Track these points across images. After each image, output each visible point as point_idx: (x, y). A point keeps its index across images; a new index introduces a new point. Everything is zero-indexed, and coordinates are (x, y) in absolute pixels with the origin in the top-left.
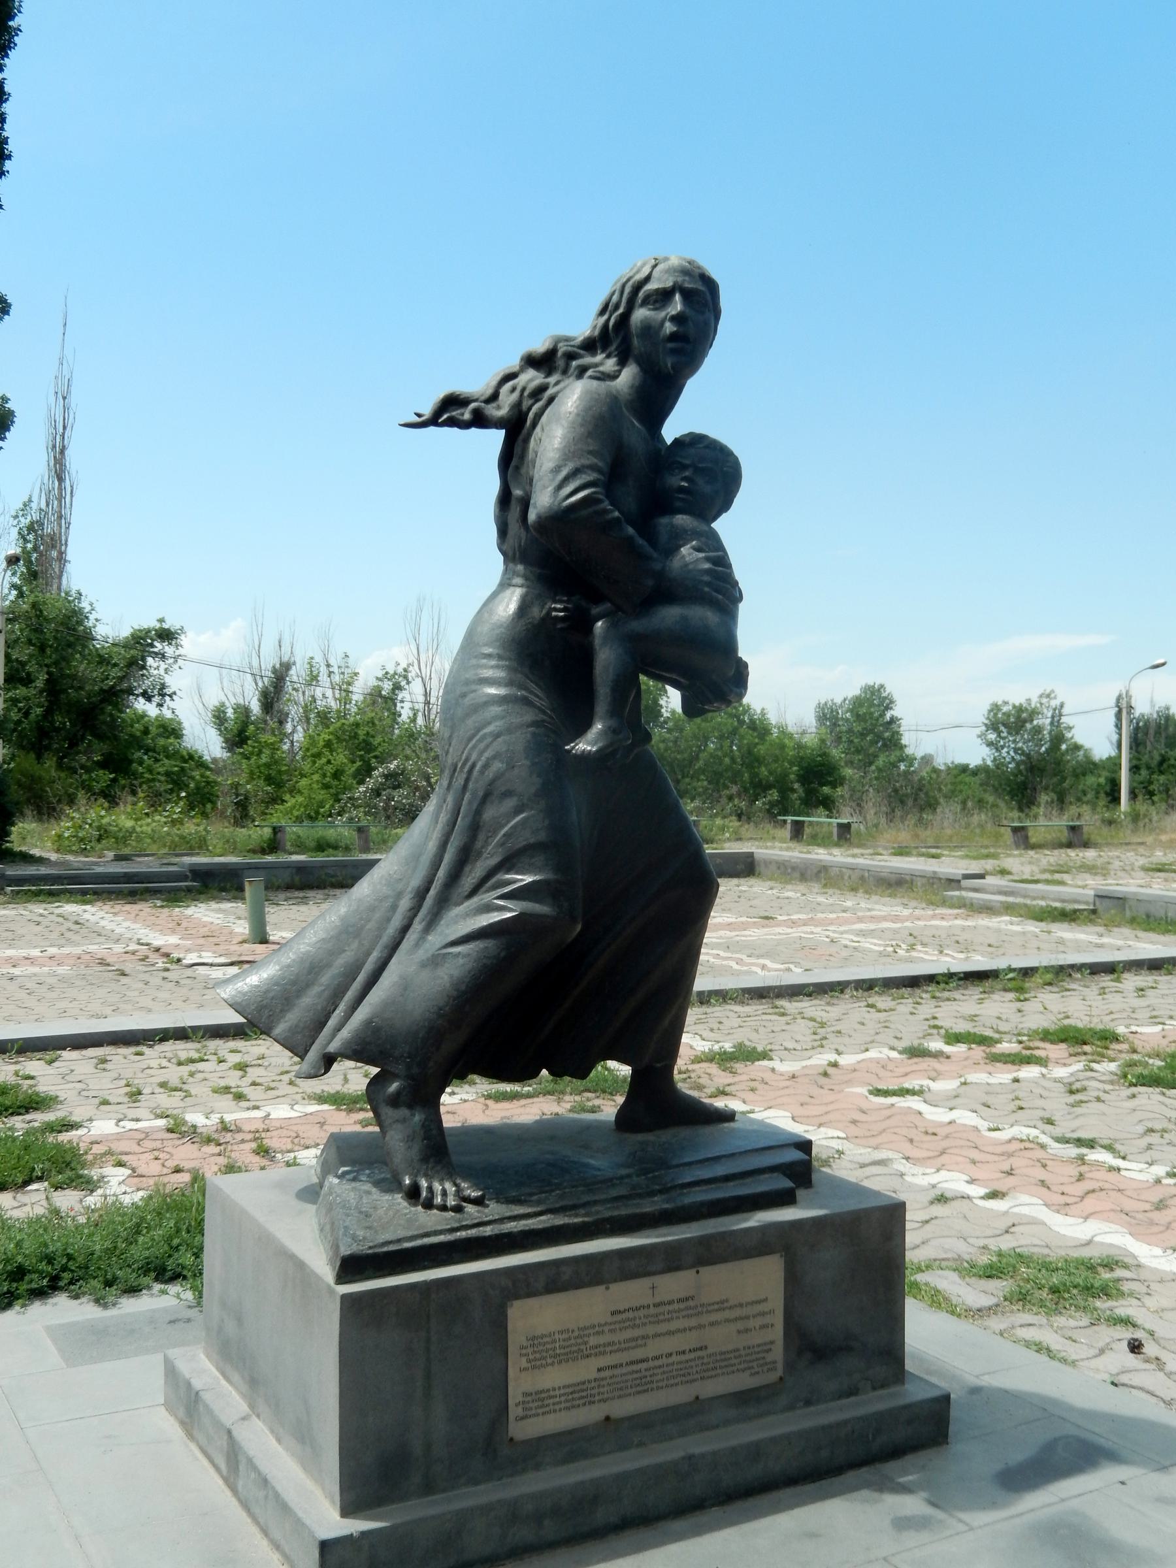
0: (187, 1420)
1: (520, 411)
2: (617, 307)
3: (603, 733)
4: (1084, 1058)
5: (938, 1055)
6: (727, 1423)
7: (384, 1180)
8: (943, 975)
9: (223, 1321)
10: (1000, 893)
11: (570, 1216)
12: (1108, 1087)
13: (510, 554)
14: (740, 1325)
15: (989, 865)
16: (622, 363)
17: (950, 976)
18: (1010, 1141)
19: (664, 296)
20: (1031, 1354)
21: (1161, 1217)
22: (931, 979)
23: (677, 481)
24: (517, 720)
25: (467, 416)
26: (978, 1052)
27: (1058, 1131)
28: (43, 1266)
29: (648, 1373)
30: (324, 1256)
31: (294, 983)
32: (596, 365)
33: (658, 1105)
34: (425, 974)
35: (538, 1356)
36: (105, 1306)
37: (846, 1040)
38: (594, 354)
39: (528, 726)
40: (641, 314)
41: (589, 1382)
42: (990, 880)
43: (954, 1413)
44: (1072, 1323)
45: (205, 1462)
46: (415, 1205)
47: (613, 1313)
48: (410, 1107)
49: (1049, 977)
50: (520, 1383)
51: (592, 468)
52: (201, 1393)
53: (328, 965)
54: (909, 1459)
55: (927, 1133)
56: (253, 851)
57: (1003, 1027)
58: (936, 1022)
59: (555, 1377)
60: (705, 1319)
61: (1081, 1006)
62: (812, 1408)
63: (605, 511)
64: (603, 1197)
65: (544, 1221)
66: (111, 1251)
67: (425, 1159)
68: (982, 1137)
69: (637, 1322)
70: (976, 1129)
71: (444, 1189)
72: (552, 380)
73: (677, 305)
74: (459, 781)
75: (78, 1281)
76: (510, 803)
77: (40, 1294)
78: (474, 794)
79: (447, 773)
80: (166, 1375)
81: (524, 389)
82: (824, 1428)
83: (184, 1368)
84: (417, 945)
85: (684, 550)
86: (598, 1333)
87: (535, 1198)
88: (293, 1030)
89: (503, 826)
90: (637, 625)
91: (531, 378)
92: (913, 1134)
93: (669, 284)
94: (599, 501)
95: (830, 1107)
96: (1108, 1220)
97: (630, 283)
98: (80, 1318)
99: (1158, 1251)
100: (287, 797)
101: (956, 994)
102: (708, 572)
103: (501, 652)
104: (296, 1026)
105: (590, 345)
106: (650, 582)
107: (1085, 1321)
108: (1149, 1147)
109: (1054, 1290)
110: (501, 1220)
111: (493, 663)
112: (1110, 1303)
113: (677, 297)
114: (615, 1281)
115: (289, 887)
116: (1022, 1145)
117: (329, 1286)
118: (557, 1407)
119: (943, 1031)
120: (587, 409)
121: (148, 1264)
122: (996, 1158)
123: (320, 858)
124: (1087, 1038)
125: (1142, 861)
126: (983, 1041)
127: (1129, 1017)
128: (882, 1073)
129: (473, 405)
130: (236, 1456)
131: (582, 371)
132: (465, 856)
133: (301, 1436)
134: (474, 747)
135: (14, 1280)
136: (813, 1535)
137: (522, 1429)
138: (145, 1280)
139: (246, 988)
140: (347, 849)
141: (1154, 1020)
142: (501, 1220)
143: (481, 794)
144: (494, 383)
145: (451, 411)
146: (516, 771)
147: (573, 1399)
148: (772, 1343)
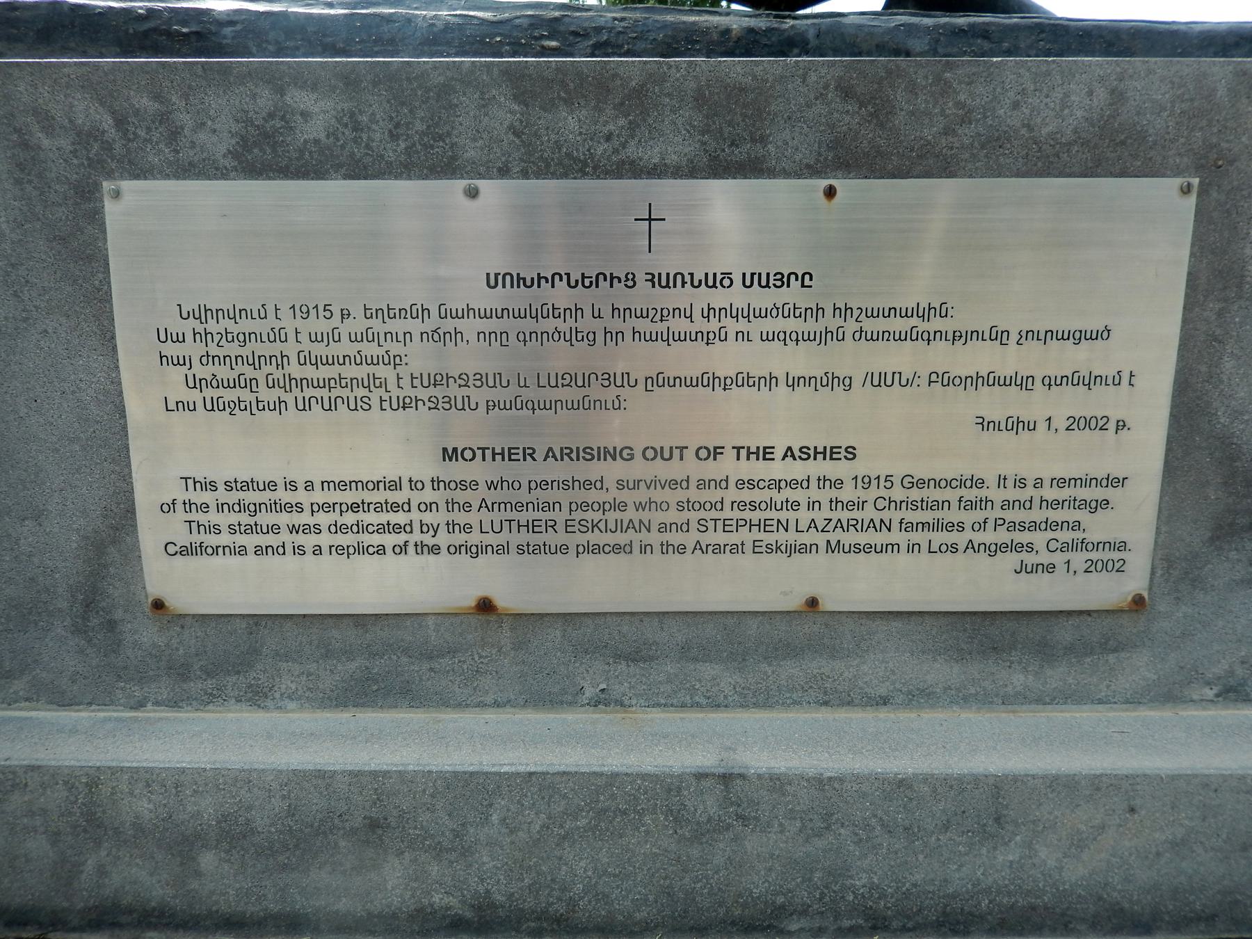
6: (920, 697)
14: (995, 404)
60: (851, 358)
69: (586, 323)
147: (361, 528)
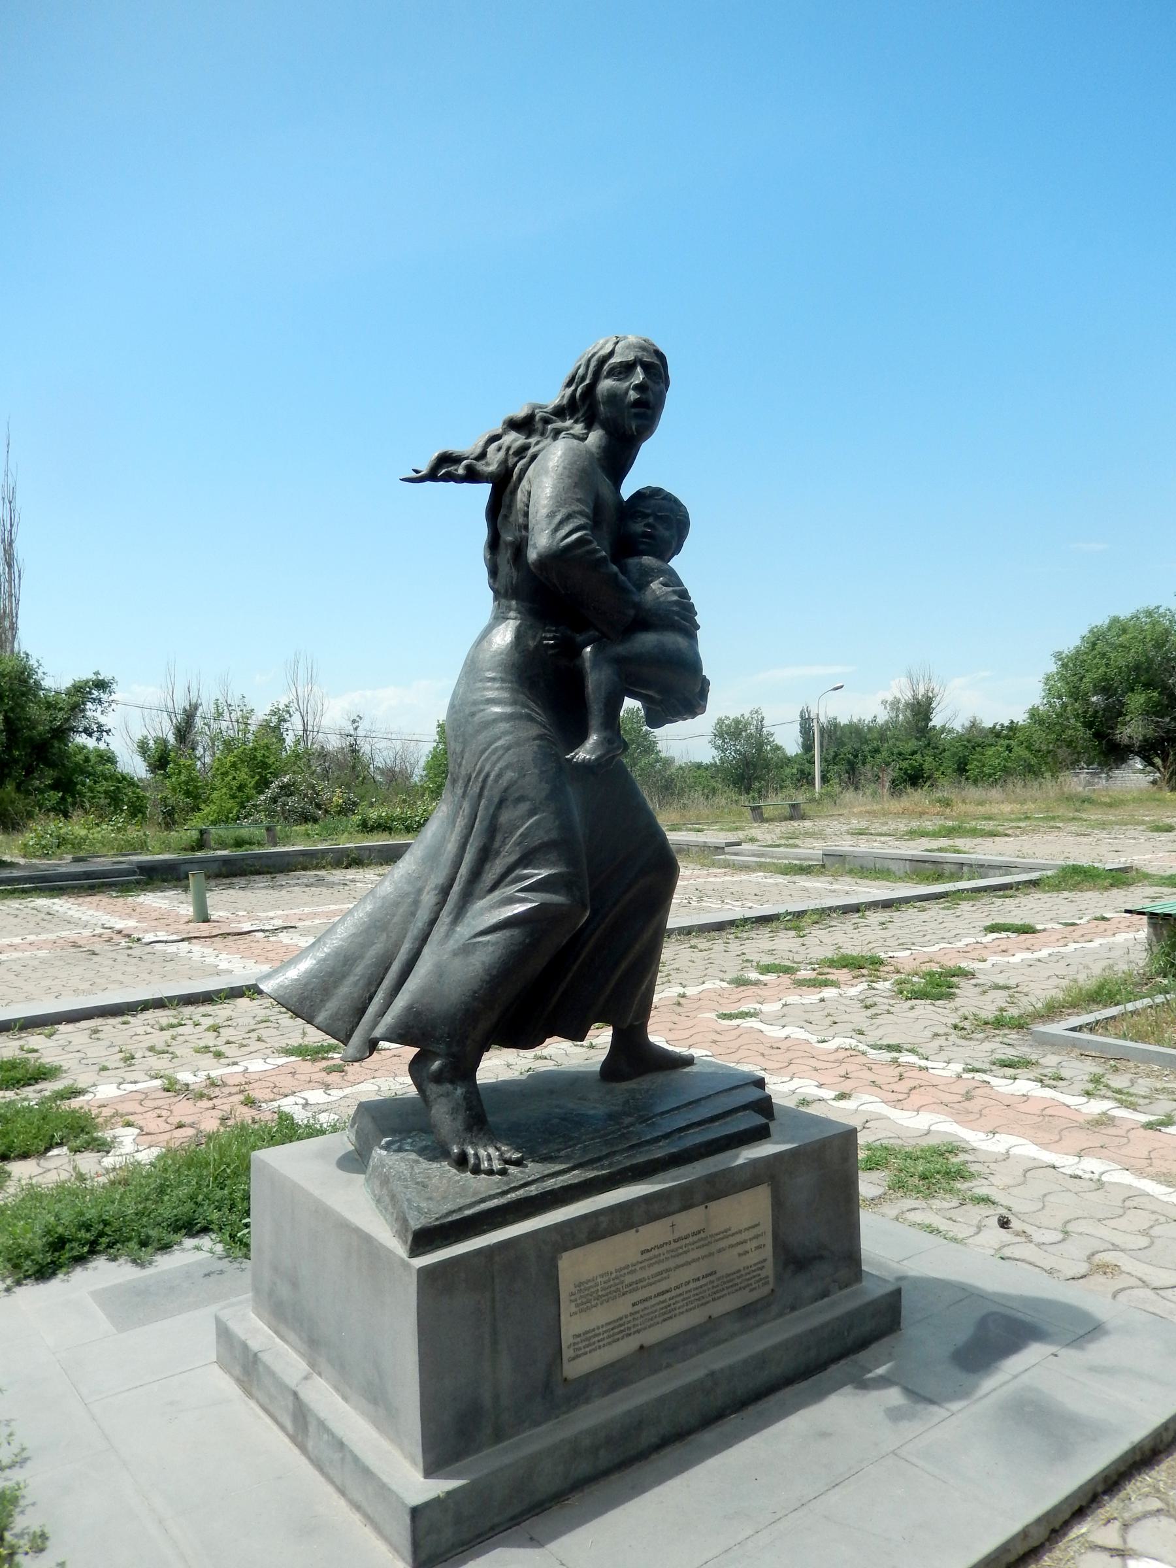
0: (245, 1379)
1: (507, 467)
2: (583, 378)
3: (596, 743)
4: (864, 979)
5: (757, 983)
6: (733, 1335)
7: (425, 1148)
8: (741, 920)
9: (275, 1284)
10: (754, 855)
11: (597, 1169)
12: (892, 1002)
13: (502, 591)
14: (740, 1249)
15: (741, 835)
16: (589, 427)
17: (745, 921)
18: (837, 1050)
19: (626, 369)
20: (925, 1235)
21: (972, 1105)
22: (732, 923)
23: (638, 527)
24: (524, 734)
25: (461, 471)
26: (786, 979)
27: (870, 1040)
28: (83, 1234)
29: (672, 1302)
30: (388, 1228)
31: (331, 974)
32: (567, 429)
33: (634, 1057)
34: (457, 962)
35: (584, 1300)
36: (142, 1266)
37: (685, 975)
38: (564, 420)
39: (534, 739)
40: (606, 384)
41: (626, 1316)
42: (745, 846)
43: (905, 1302)
44: (946, 1205)
45: (268, 1421)
46: (464, 1171)
47: (642, 1253)
48: (452, 1082)
49: (815, 917)
50: (572, 1325)
51: (581, 513)
52: (260, 1354)
53: (361, 957)
54: (875, 1348)
55: (772, 1047)
56: (185, 850)
57: (798, 958)
58: (746, 957)
59: (599, 1317)
60: (714, 1248)
61: (847, 938)
62: (797, 1313)
63: (595, 551)
64: (620, 1147)
65: (578, 1175)
66: (140, 1214)
67: (469, 1128)
68: (814, 1048)
69: (662, 1257)
70: (808, 1042)
71: (488, 1154)
72: (533, 440)
73: (639, 376)
74: (474, 789)
75: (114, 1244)
76: (524, 807)
77: (80, 1260)
78: (490, 800)
79: (460, 783)
80: (219, 1335)
81: (509, 448)
82: (812, 1331)
83: (238, 1329)
84: (448, 936)
85: (654, 585)
86: (630, 1273)
87: (563, 1153)
88: (334, 1017)
89: (518, 828)
90: (620, 649)
91: (513, 439)
92: (761, 1048)
93: (631, 358)
94: (590, 542)
95: (692, 1031)
96: (933, 1111)
97: (596, 357)
98: (120, 1280)
99: (982, 1136)
100: (203, 806)
101: (752, 934)
102: (676, 603)
103: (499, 675)
104: (337, 1013)
105: (560, 412)
106: (632, 612)
107: (955, 1203)
108: (941, 1049)
109: (924, 1177)
110: (542, 1179)
111: (497, 685)
112: (967, 1185)
113: (639, 369)
114: (643, 1224)
115: (218, 876)
116: (849, 1053)
117: (403, 1260)
118: (601, 1344)
119: (754, 964)
120: (572, 463)
121: (177, 1221)
122: (832, 1065)
123: (240, 852)
124: (862, 963)
125: (845, 828)
126: (787, 970)
127: (883, 946)
128: (721, 1001)
129: (465, 462)
130: (305, 1417)
131: (557, 433)
132: (485, 855)
133: (374, 1397)
134: (487, 759)
135: (55, 1250)
136: (824, 1435)
137: (574, 1369)
138: (176, 1237)
139: (287, 982)
140: (260, 844)
141: (902, 946)
142: (542, 1179)
143: (496, 800)
144: (482, 443)
145: (445, 468)
146: (527, 779)
147: (614, 1335)
148: (765, 1260)
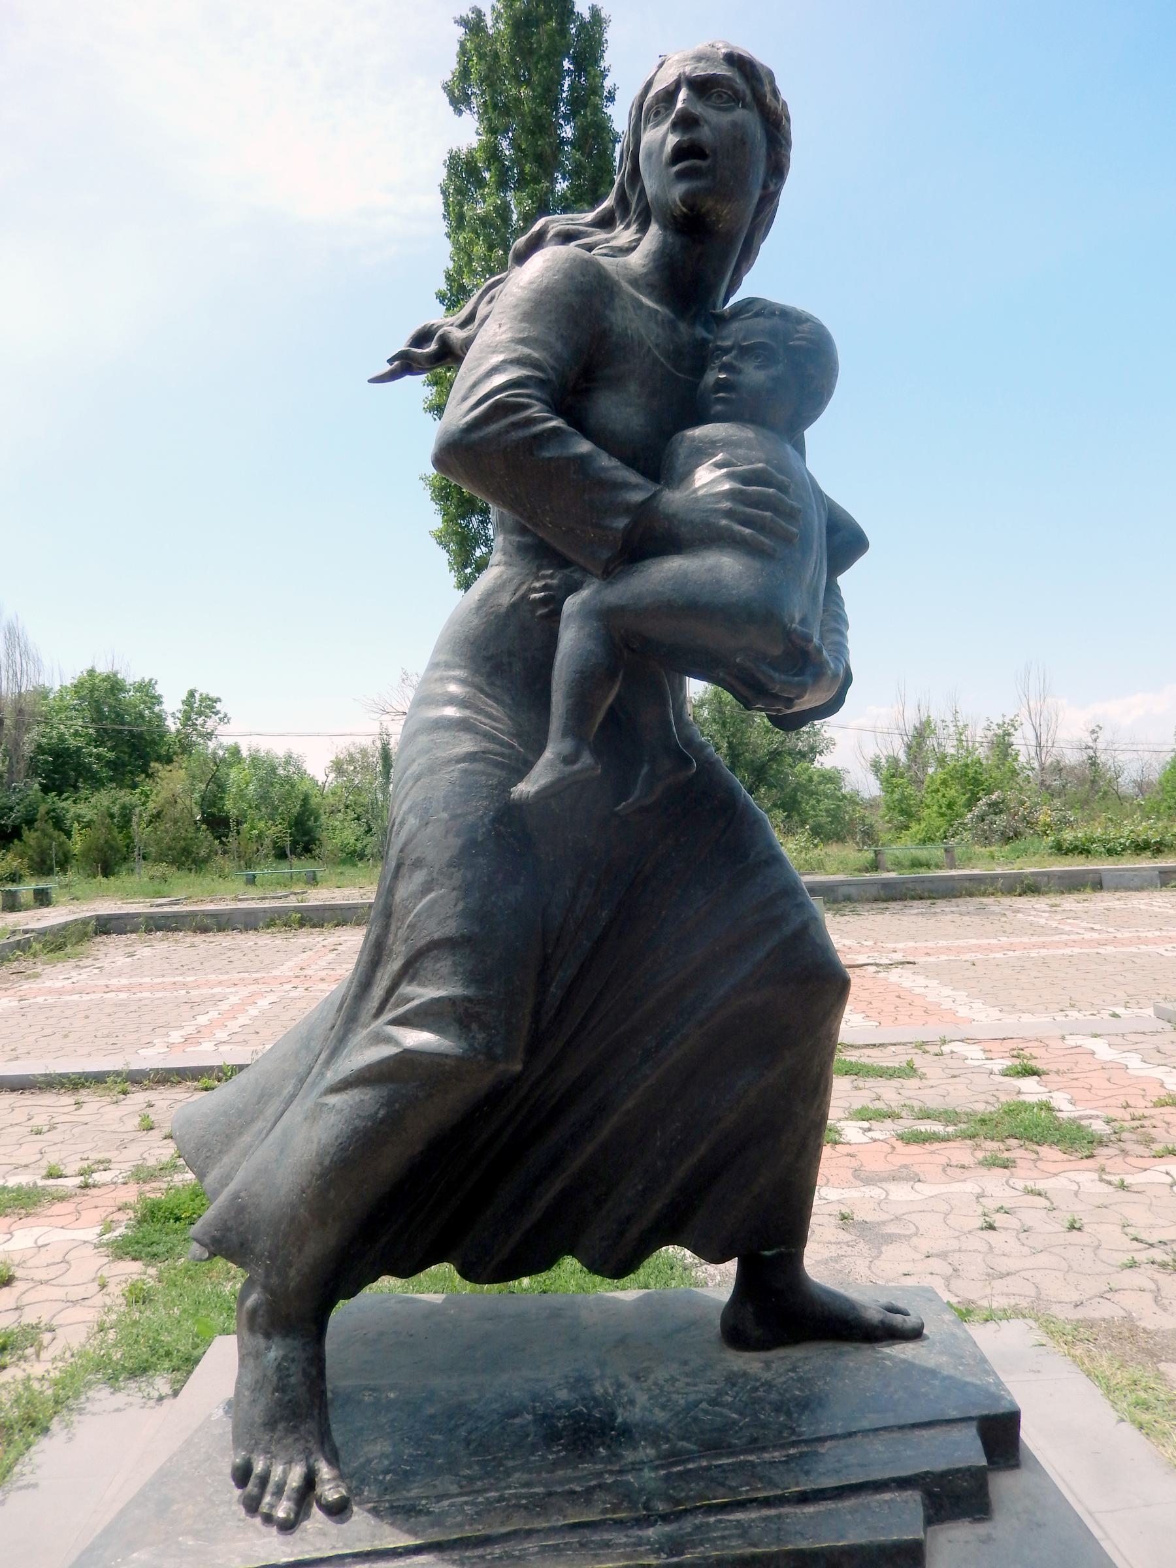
33: (781, 1309)
39: (458, 761)
51: (518, 362)
56: (859, 871)
63: (531, 421)
76: (420, 877)
100: (913, 825)
123: (908, 874)
140: (938, 867)
146: (429, 829)
